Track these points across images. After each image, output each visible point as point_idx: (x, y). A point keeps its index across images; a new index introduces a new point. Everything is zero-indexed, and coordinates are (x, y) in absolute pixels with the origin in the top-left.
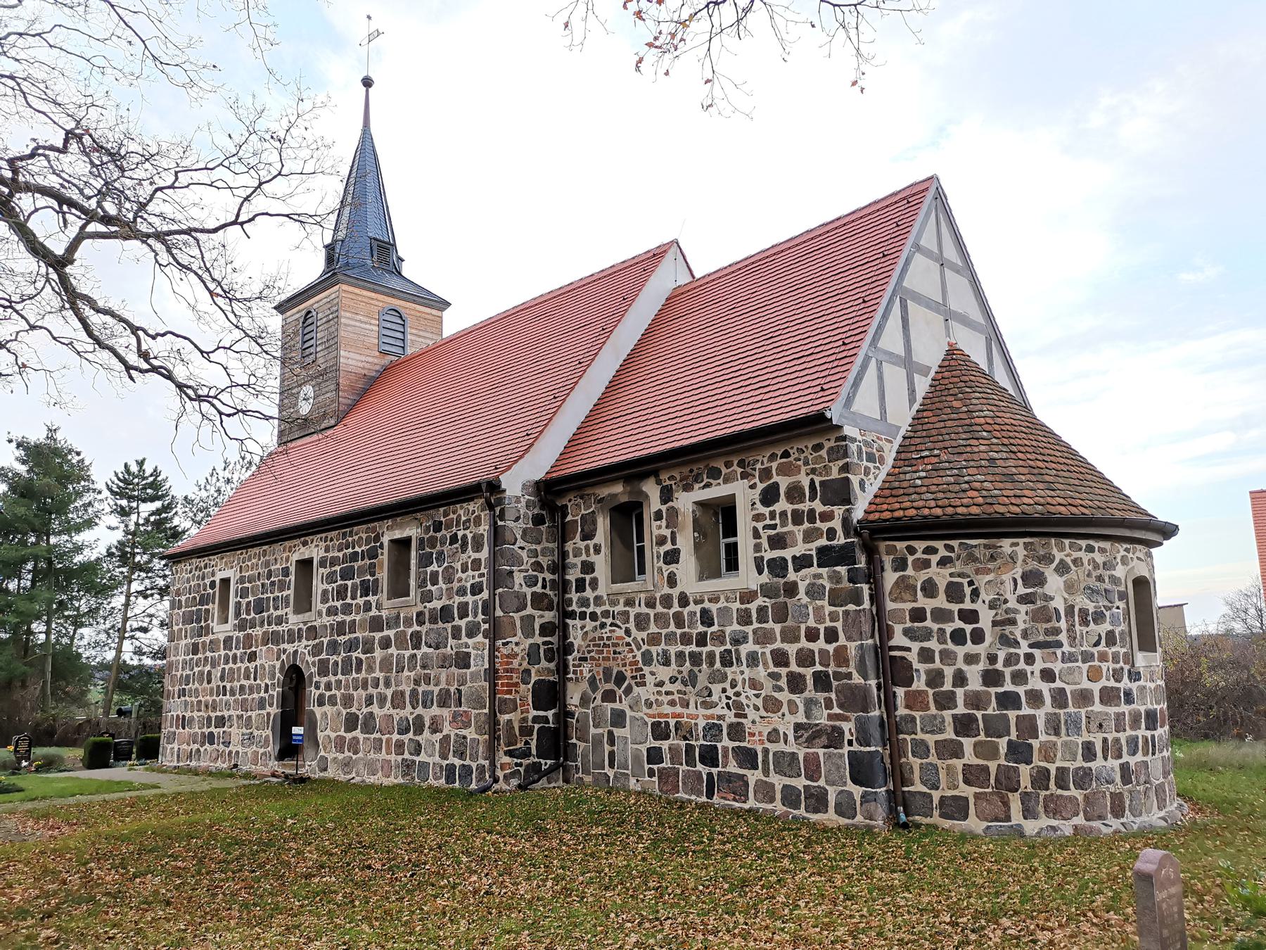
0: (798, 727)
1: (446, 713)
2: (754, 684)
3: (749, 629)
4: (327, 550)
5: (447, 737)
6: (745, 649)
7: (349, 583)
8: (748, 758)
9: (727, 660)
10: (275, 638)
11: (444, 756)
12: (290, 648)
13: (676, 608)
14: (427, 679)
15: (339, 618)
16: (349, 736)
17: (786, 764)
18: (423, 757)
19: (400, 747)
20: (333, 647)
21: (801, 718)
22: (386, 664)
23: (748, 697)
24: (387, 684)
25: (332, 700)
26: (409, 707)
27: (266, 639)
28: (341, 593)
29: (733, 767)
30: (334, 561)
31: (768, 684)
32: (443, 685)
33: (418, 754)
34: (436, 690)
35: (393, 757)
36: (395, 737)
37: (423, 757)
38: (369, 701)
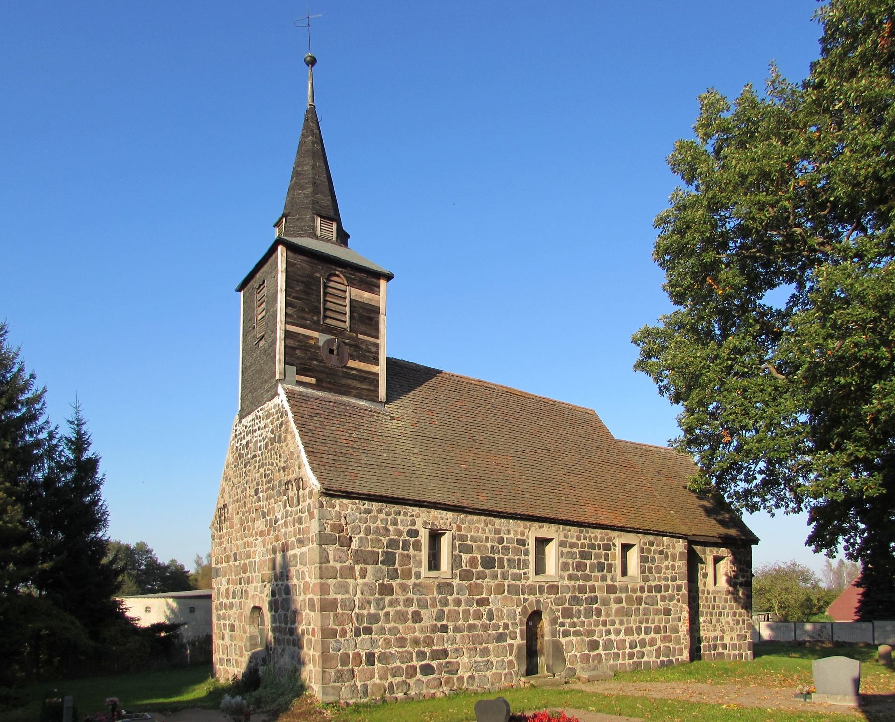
0: (738, 636)
1: (658, 636)
2: (728, 623)
3: (727, 605)
4: (566, 536)
5: (660, 648)
6: (726, 611)
7: (588, 562)
8: (725, 647)
9: (720, 615)
10: (513, 590)
11: (658, 657)
12: (531, 598)
13: (706, 594)
14: (647, 621)
15: (581, 582)
16: (592, 654)
17: (734, 647)
18: (646, 659)
19: (631, 656)
20: (576, 600)
21: (738, 633)
22: (620, 612)
23: (727, 627)
24: (621, 623)
25: (577, 633)
26: (636, 635)
27: (500, 590)
28: (580, 567)
29: (721, 650)
30: (573, 546)
31: (732, 622)
32: (656, 623)
33: (643, 657)
34: (653, 626)
35: (627, 661)
36: (628, 651)
37: (646, 659)
38: (608, 632)
